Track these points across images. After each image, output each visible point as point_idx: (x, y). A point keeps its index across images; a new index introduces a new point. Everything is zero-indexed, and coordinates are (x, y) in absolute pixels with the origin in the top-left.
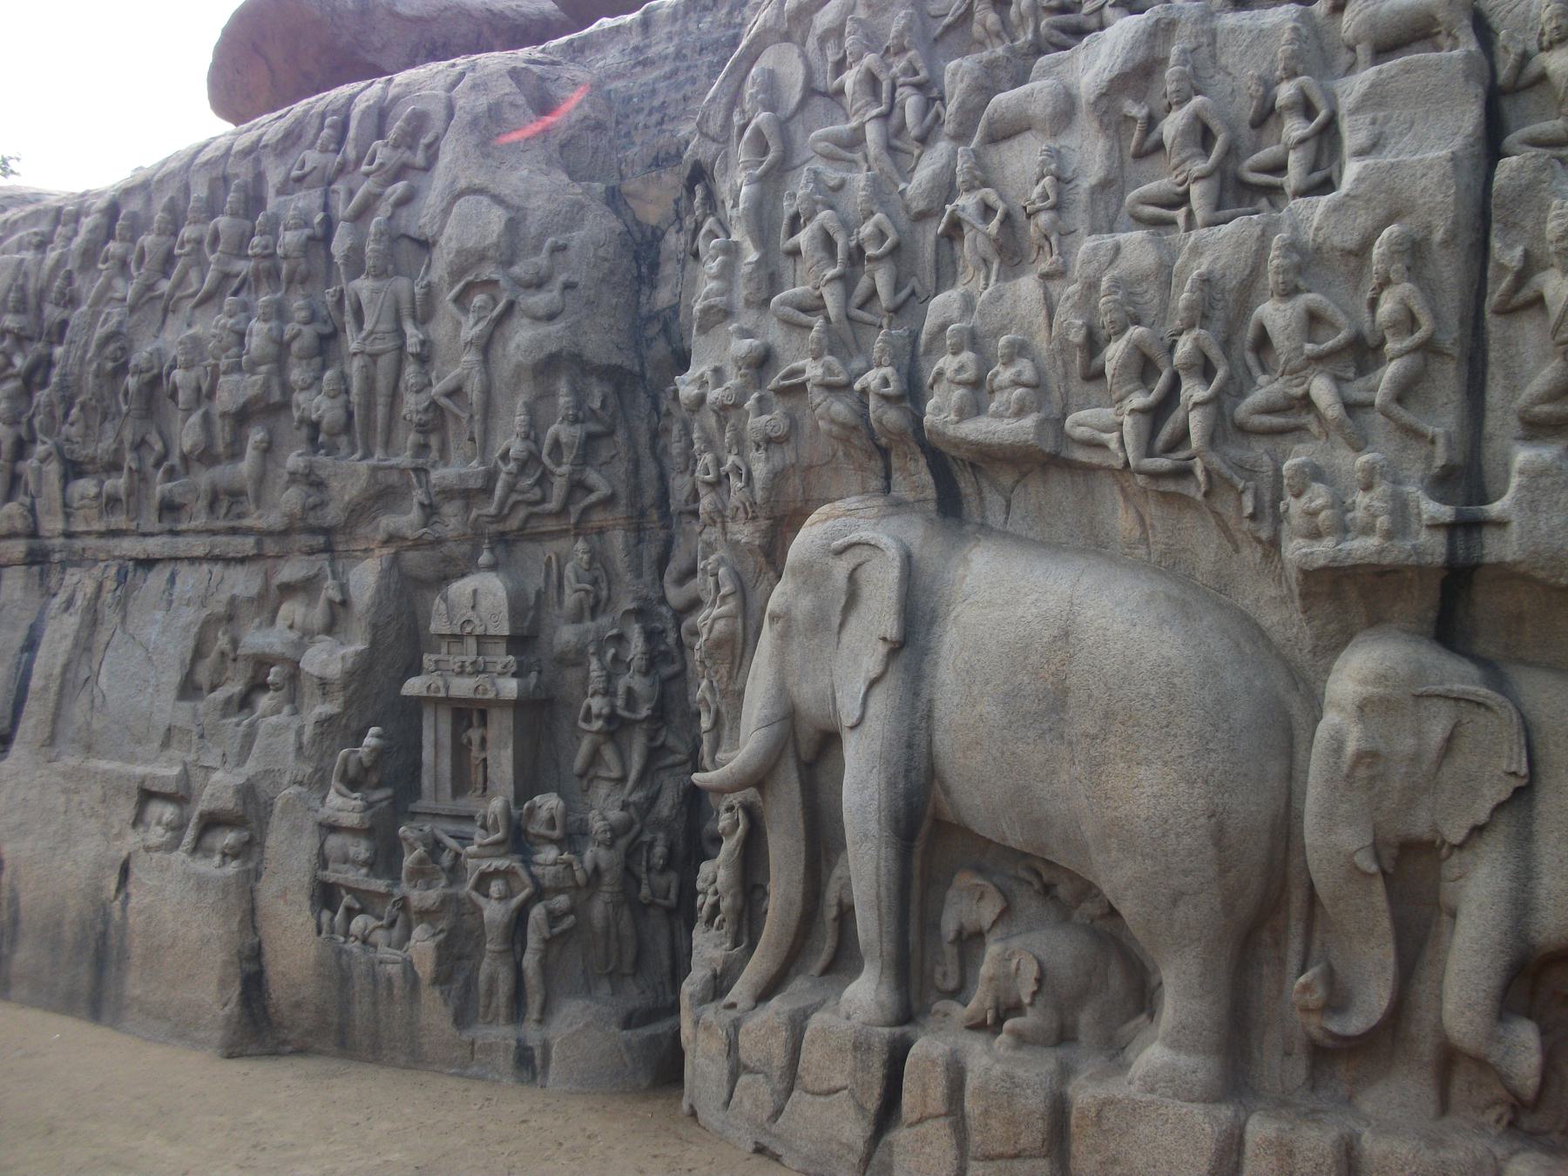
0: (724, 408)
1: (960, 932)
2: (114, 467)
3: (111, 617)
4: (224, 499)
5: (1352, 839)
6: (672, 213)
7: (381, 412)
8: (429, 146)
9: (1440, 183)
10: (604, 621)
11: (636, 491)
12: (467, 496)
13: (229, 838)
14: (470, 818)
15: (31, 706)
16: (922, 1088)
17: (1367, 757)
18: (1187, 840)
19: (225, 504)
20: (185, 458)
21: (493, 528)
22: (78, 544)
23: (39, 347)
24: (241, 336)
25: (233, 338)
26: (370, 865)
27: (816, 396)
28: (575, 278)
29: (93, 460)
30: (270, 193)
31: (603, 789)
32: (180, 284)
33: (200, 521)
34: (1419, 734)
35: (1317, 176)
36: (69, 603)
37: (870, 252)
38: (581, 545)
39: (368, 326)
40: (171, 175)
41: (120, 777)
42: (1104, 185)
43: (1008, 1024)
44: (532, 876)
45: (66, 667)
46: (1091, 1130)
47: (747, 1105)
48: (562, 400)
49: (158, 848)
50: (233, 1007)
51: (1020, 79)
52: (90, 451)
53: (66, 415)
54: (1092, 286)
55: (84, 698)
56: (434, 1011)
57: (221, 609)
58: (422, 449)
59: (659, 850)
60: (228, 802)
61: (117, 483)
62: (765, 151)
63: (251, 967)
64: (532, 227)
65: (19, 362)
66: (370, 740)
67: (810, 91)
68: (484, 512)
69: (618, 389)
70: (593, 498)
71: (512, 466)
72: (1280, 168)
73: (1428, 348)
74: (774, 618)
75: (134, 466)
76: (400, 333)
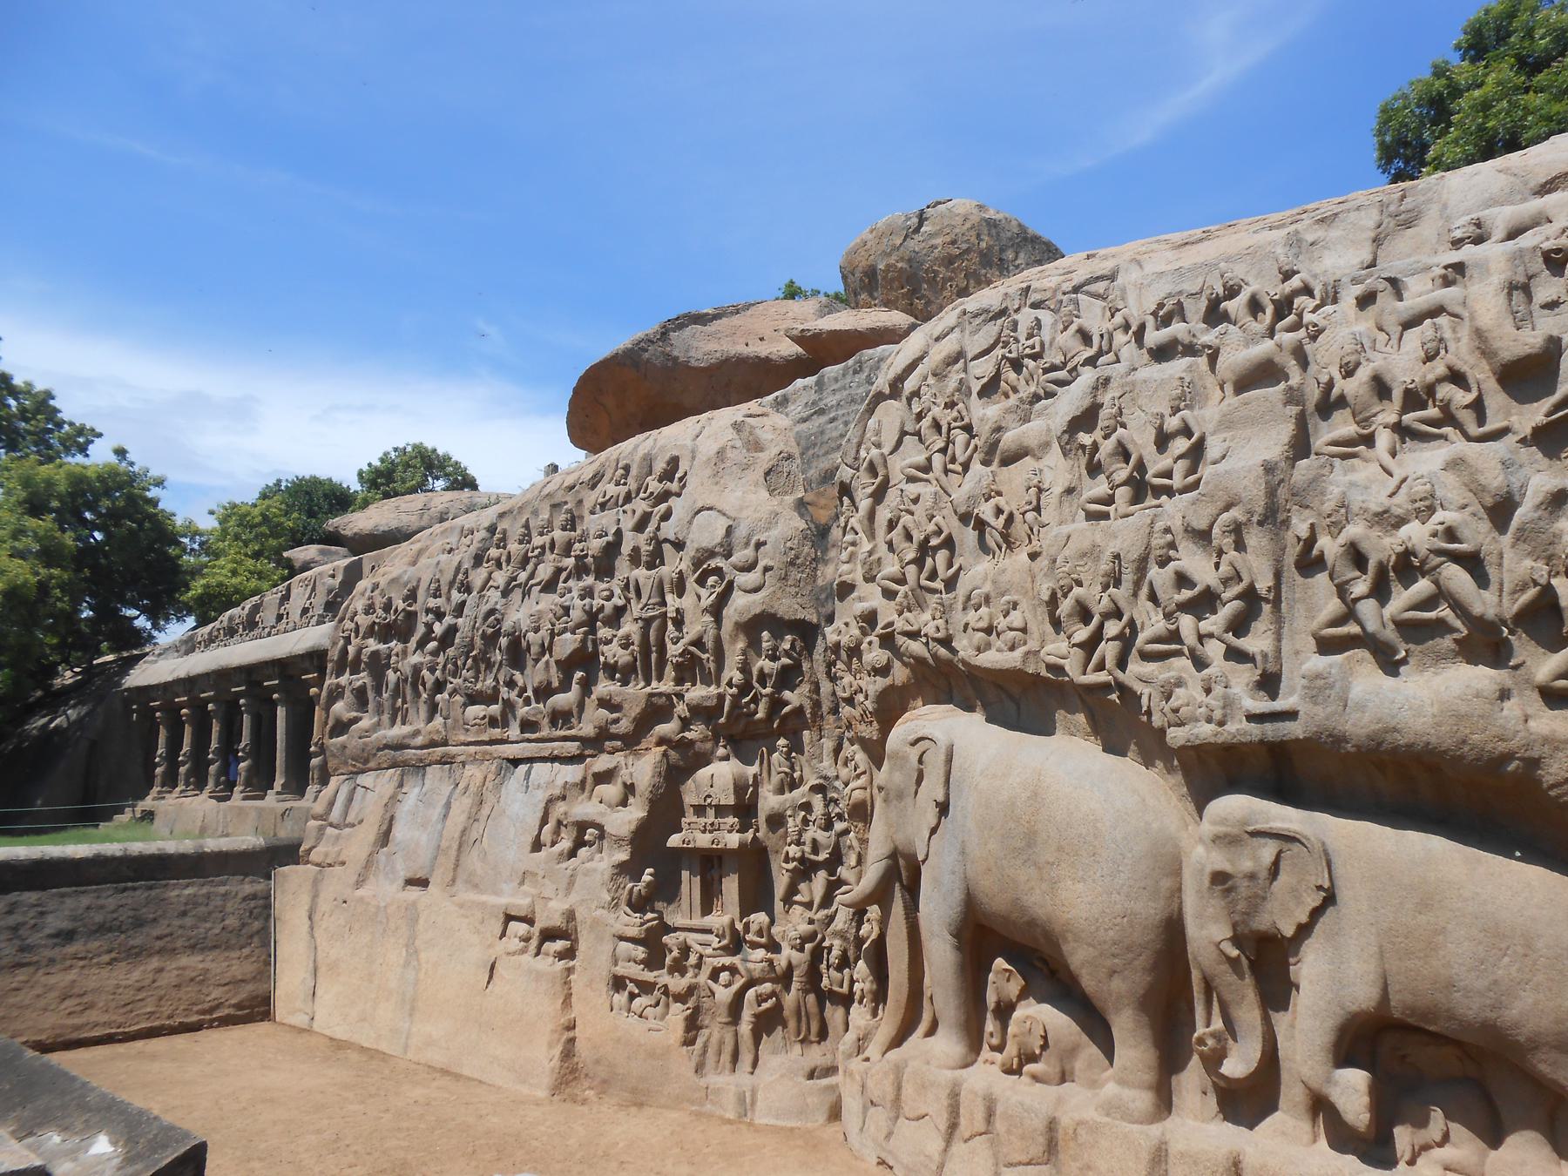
0: (849, 648)
1: (998, 1003)
3: (490, 798)
4: (560, 718)
5: (1220, 931)
7: (654, 656)
8: (681, 479)
9: (1255, 482)
10: (796, 793)
11: (817, 705)
13: (560, 945)
14: (709, 931)
15: (441, 859)
16: (971, 1118)
17: (1220, 878)
18: (1111, 933)
20: (536, 691)
22: (472, 749)
23: (448, 620)
24: (566, 610)
25: (561, 612)
26: (642, 962)
27: (900, 640)
28: (771, 563)
30: (586, 513)
31: (797, 909)
32: (532, 576)
33: (545, 732)
34: (1255, 858)
35: (1191, 479)
36: (467, 788)
37: (934, 542)
38: (782, 742)
39: (644, 600)
42: (1070, 491)
43: (1026, 1069)
44: (748, 970)
45: (464, 832)
46: (1072, 1144)
47: (872, 1129)
48: (764, 645)
49: (514, 954)
50: (556, 1062)
51: (1026, 419)
52: (479, 686)
54: (1055, 561)
55: (475, 852)
56: (683, 1062)
57: (557, 792)
58: (679, 681)
59: (836, 952)
60: (557, 921)
61: (495, 709)
62: (876, 475)
63: (571, 1034)
64: (741, 533)
65: (438, 629)
66: (646, 878)
67: (903, 433)
69: (803, 638)
70: (787, 709)
72: (1168, 474)
73: (1251, 597)
74: (880, 789)
76: (664, 603)
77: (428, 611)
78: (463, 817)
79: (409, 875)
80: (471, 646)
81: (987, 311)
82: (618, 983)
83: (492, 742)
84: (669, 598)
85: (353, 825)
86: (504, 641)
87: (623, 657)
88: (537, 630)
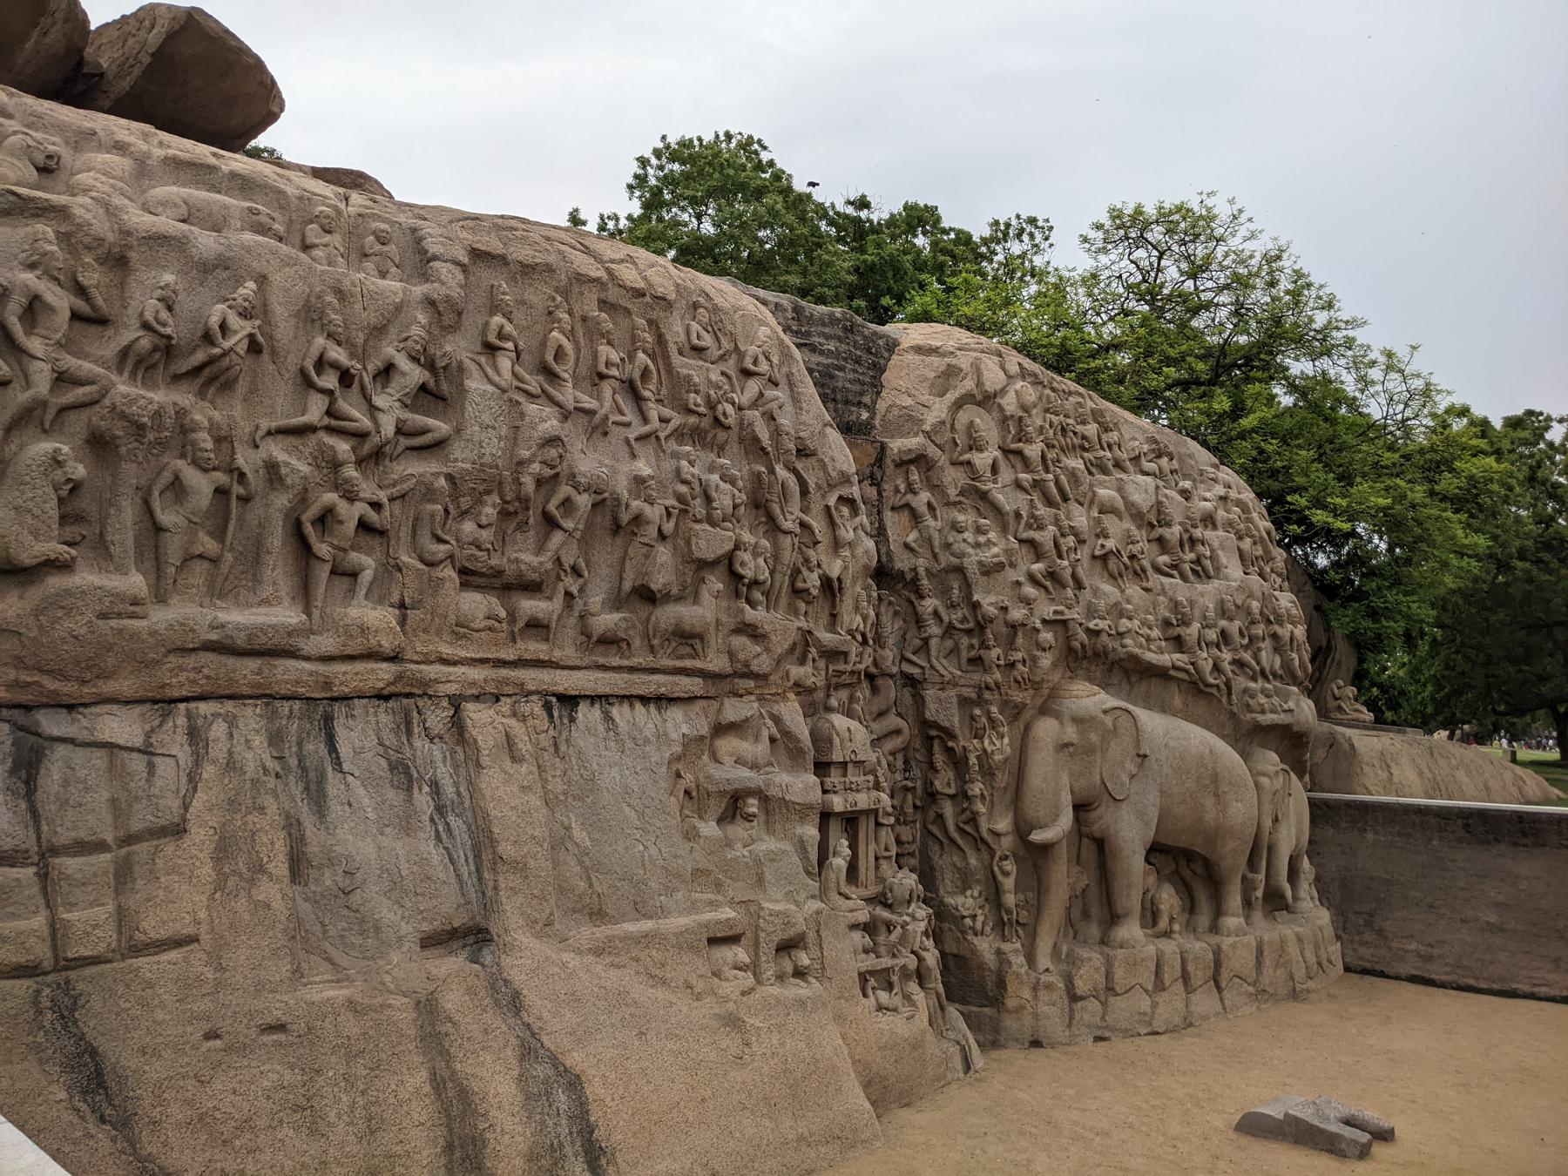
2: (532, 588)
6: (868, 471)
12: (833, 655)
13: (804, 959)
19: (674, 644)
21: (835, 680)
29: (499, 573)
30: (673, 349)
40: (549, 269)
41: (675, 935)
52: (493, 562)
53: (464, 514)
57: (678, 749)
68: (841, 667)
71: (859, 638)
74: (1066, 745)
75: (575, 592)
77: (321, 364)
78: (535, 801)
79: (425, 927)
80: (488, 482)
81: (1036, 376)
82: (863, 977)
83: (520, 663)
84: (806, 518)
85: (101, 847)
86: (584, 501)
87: (765, 575)
88: (650, 501)
